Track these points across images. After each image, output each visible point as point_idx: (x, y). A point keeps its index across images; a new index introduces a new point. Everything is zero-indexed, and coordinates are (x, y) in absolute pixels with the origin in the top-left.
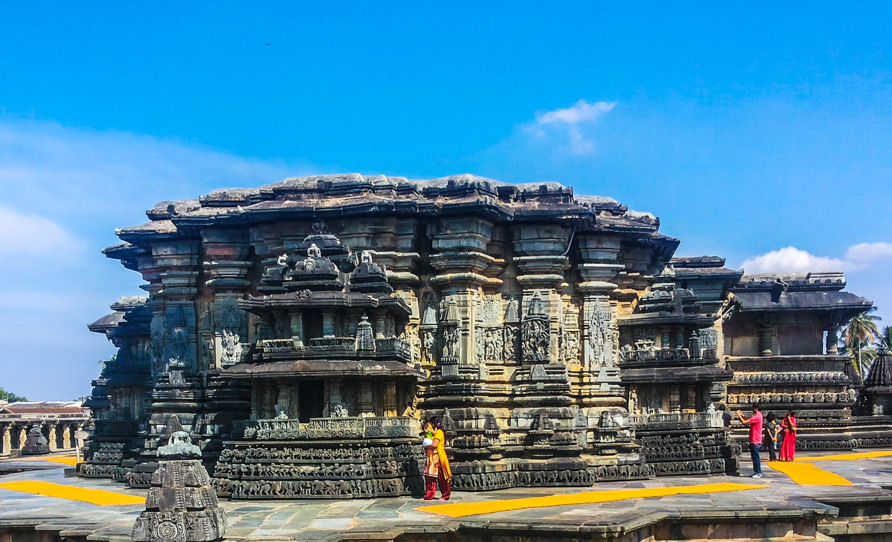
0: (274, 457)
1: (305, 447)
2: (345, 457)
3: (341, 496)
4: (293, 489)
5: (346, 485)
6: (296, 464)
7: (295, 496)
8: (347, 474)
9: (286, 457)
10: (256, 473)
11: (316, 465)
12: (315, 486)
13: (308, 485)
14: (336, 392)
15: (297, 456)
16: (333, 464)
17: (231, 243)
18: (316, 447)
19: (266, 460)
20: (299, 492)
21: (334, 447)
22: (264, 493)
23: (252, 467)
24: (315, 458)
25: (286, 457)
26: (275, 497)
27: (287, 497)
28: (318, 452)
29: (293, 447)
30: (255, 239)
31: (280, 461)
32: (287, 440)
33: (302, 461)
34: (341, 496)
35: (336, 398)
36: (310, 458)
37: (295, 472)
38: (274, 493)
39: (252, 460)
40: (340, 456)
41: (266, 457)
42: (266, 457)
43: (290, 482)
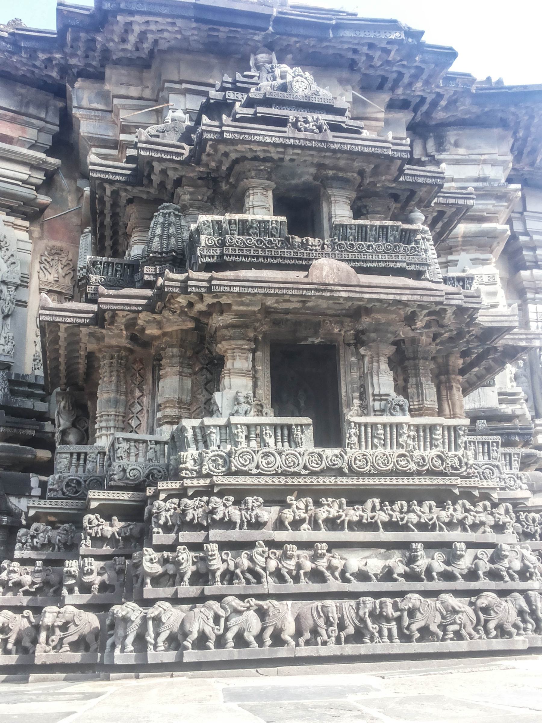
0: (258, 525)
1: (356, 497)
2: (475, 527)
3: (498, 644)
4: (342, 627)
5: (507, 610)
6: (333, 546)
7: (350, 649)
8: (494, 575)
9: (296, 524)
10: (202, 577)
11: (389, 546)
12: (412, 613)
13: (390, 610)
14: (384, 366)
15: (333, 524)
16: (444, 546)
17: (18, 116)
18: (389, 496)
19: (235, 535)
20: (358, 636)
21: (442, 497)
22: (241, 641)
23: (186, 557)
24: (391, 526)
25: (296, 524)
26: (282, 652)
27: (323, 651)
28: (395, 511)
29: (317, 495)
30: (85, 103)
31: (280, 536)
32: (284, 474)
33: (346, 536)
34: (498, 644)
35: (384, 382)
36: (372, 526)
37: (331, 568)
38: (278, 640)
39: (186, 536)
40: (461, 523)
41: (230, 524)
42: (230, 524)
43: (331, 604)
